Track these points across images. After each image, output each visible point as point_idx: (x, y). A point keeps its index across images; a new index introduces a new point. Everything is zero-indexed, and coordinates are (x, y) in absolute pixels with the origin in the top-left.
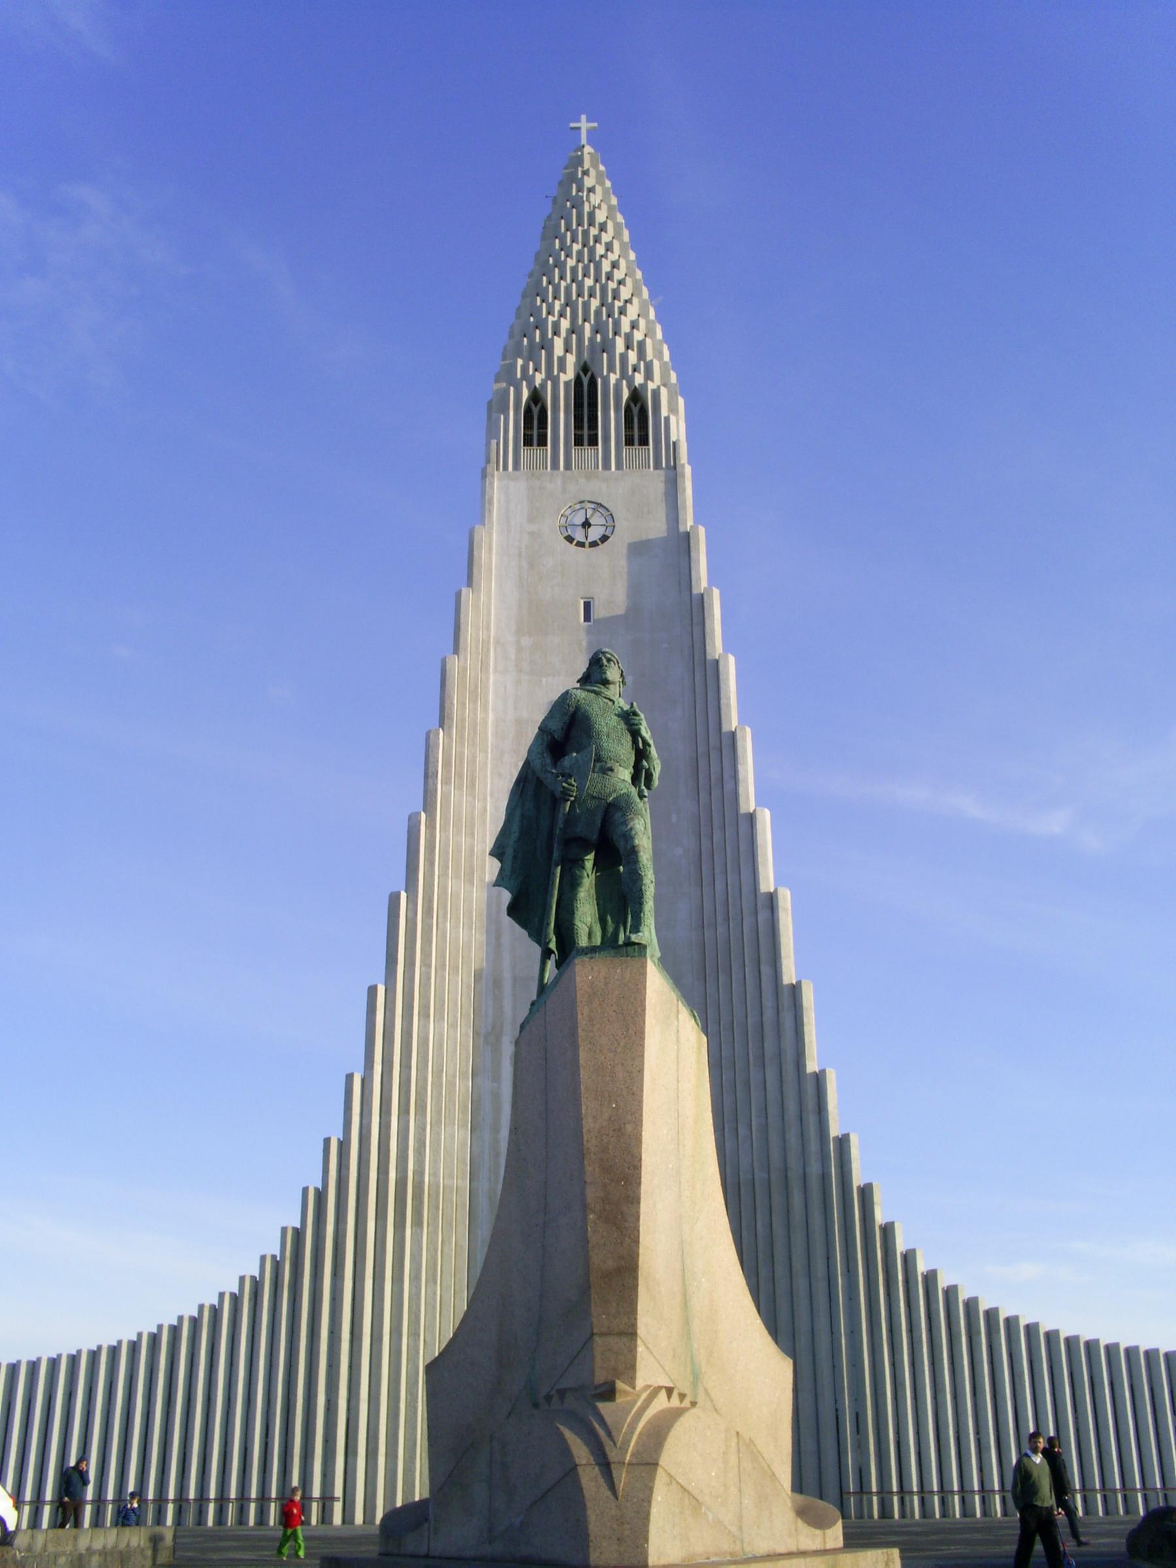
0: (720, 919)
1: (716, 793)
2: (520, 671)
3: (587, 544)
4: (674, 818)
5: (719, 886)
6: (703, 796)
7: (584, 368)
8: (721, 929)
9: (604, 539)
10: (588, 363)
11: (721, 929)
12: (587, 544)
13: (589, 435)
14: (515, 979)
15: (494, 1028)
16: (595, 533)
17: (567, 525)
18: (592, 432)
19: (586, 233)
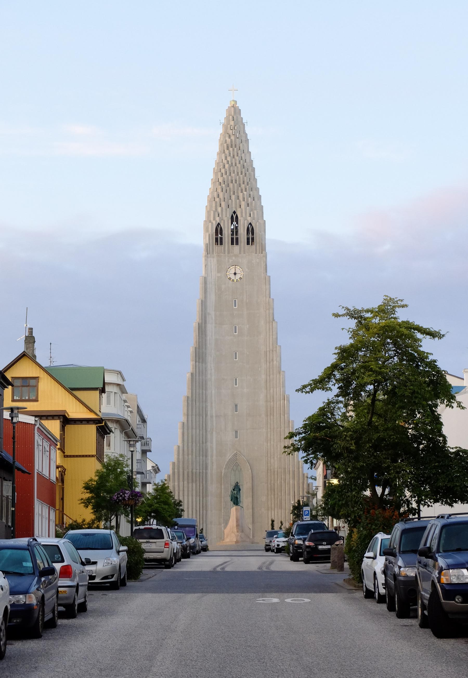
0: (271, 401)
1: (271, 363)
2: (216, 323)
3: (235, 281)
4: (260, 370)
5: (271, 391)
6: (268, 364)
7: (234, 212)
8: (272, 403)
9: (240, 278)
10: (235, 211)
11: (272, 403)
12: (235, 281)
13: (236, 238)
14: (216, 416)
15: (211, 429)
16: (238, 277)
17: (229, 274)
18: (237, 237)
19: (233, 150)
